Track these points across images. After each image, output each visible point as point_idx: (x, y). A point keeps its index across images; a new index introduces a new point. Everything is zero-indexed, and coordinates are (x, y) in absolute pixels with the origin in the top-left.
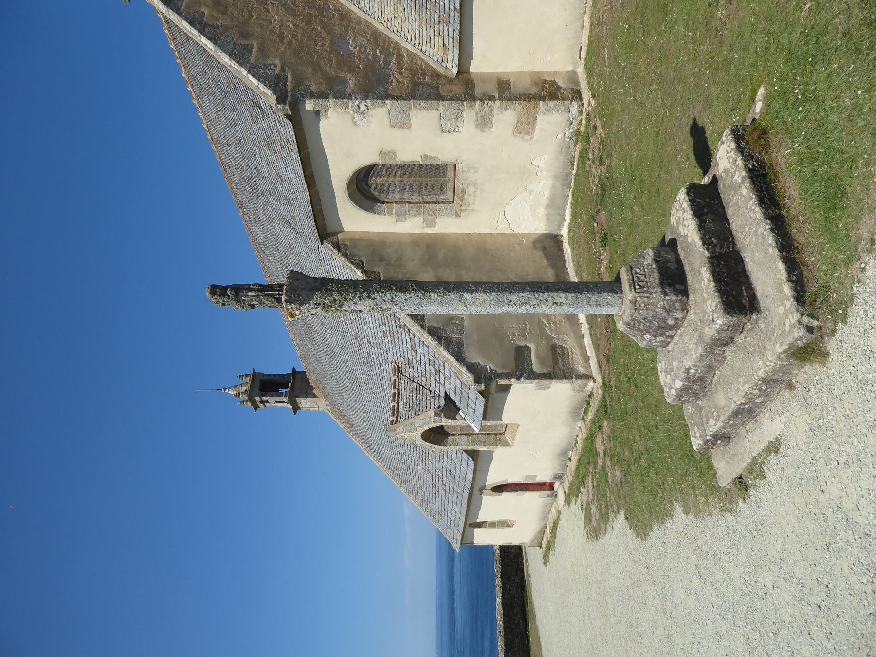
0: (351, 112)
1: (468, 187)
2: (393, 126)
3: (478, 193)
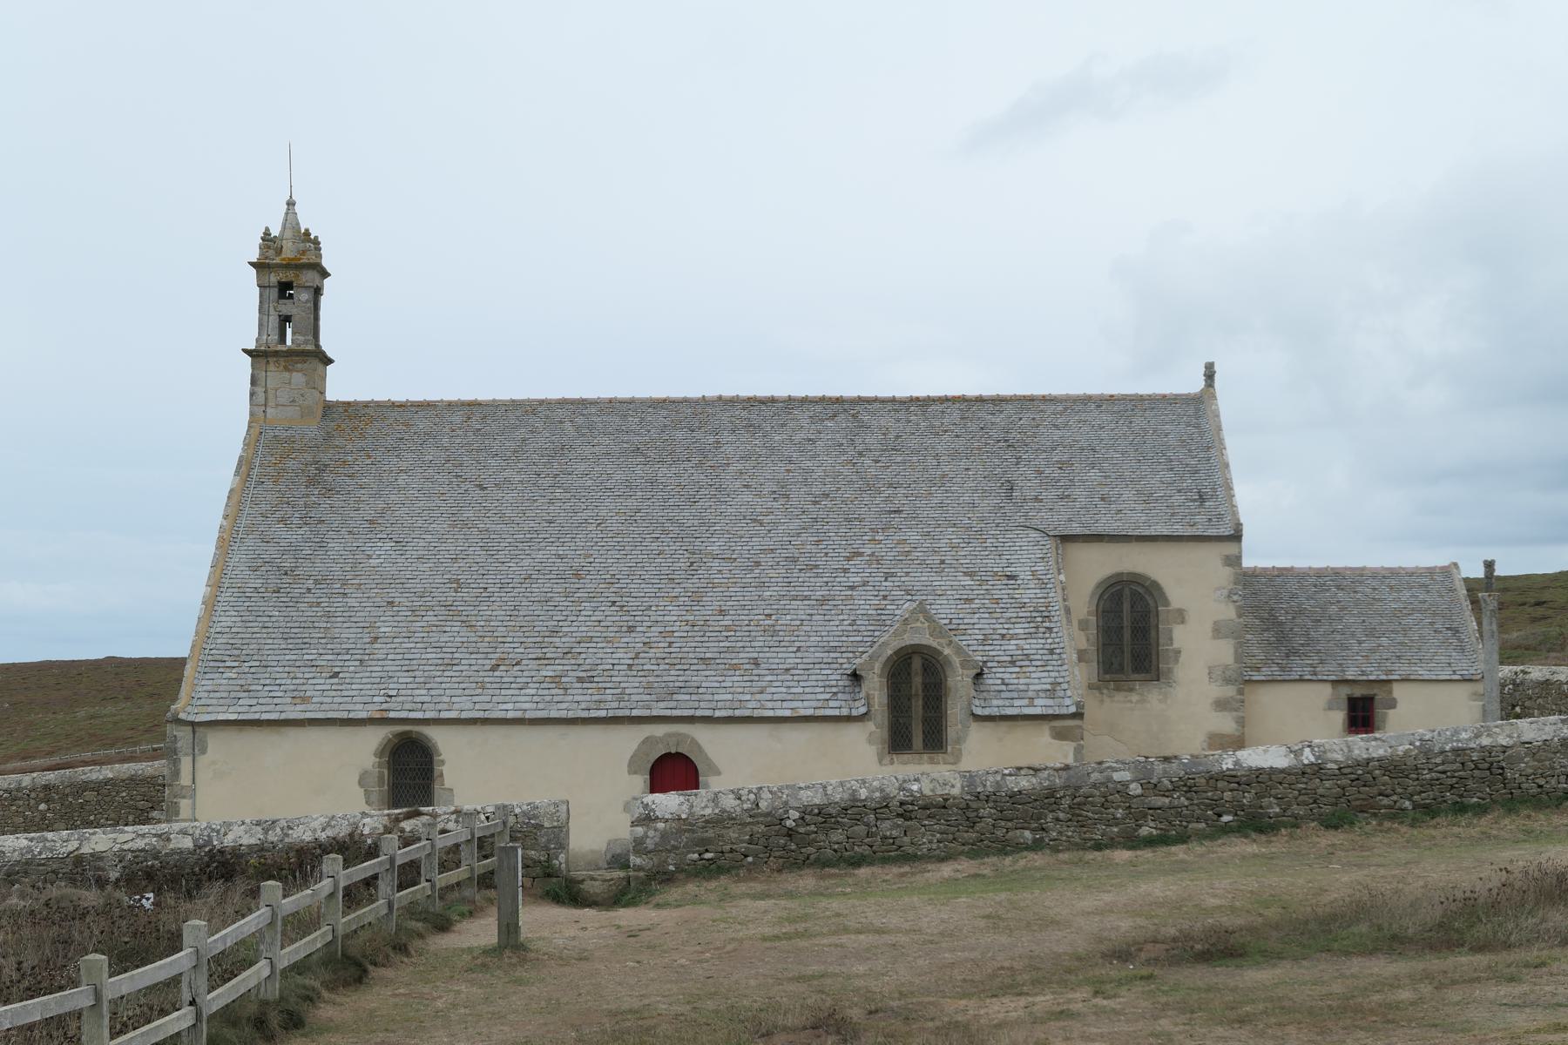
0: (1230, 588)
1: (1138, 694)
2: (1215, 623)
3: (1129, 705)
